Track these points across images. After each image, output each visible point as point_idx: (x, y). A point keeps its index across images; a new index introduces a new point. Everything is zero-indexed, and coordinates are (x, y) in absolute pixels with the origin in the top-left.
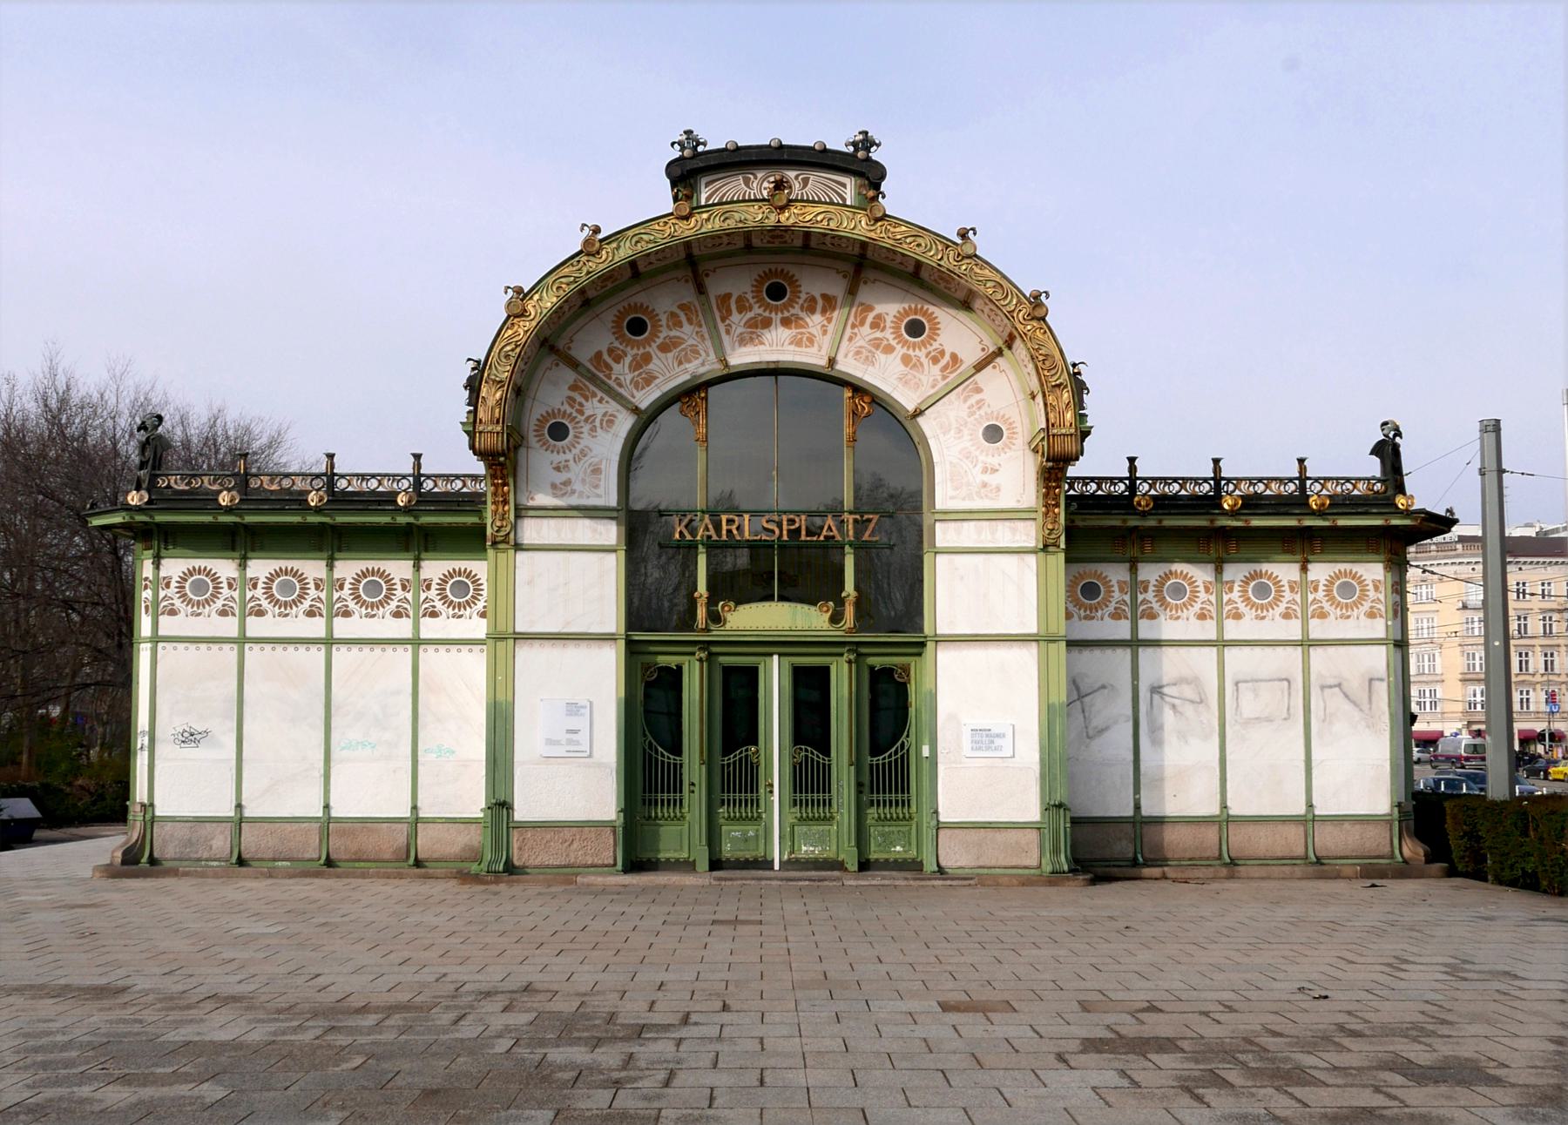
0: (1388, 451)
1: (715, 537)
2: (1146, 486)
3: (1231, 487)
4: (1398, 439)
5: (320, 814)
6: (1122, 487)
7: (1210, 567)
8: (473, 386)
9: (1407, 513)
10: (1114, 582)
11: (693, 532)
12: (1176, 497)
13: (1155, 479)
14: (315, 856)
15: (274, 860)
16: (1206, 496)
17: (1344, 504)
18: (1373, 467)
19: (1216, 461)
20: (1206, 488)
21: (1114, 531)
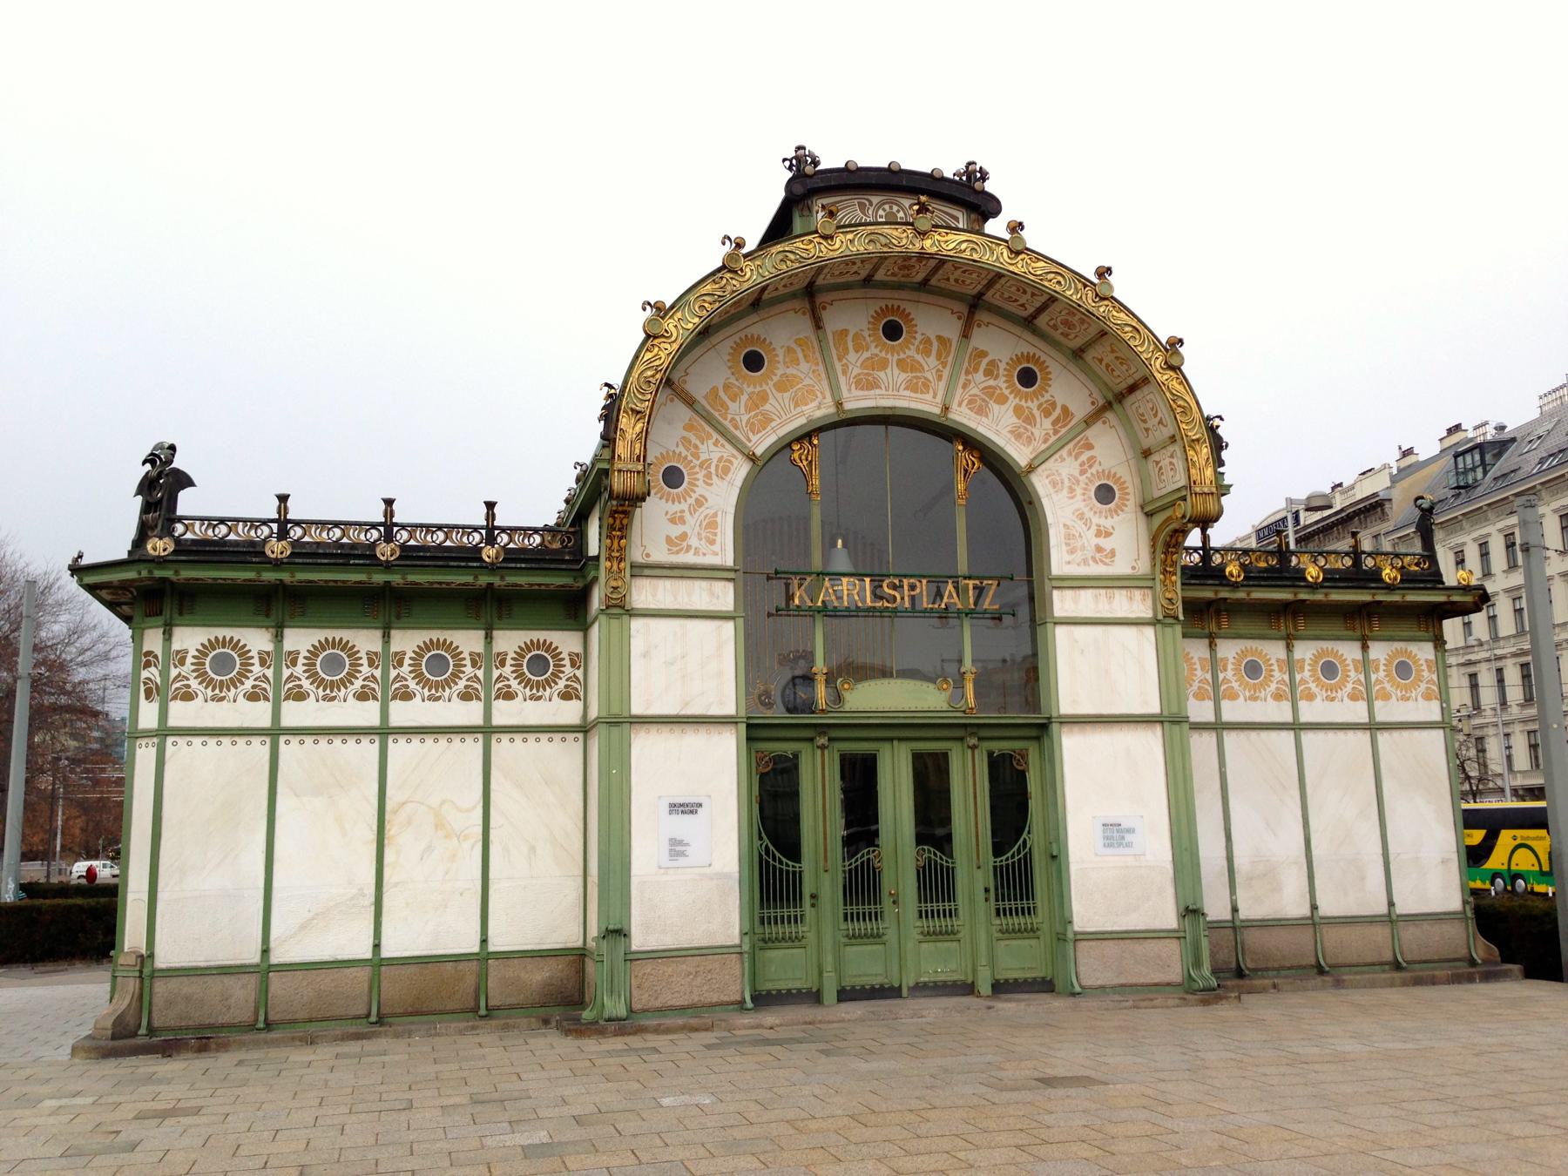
7: (1281, 645)
10: (1195, 660)
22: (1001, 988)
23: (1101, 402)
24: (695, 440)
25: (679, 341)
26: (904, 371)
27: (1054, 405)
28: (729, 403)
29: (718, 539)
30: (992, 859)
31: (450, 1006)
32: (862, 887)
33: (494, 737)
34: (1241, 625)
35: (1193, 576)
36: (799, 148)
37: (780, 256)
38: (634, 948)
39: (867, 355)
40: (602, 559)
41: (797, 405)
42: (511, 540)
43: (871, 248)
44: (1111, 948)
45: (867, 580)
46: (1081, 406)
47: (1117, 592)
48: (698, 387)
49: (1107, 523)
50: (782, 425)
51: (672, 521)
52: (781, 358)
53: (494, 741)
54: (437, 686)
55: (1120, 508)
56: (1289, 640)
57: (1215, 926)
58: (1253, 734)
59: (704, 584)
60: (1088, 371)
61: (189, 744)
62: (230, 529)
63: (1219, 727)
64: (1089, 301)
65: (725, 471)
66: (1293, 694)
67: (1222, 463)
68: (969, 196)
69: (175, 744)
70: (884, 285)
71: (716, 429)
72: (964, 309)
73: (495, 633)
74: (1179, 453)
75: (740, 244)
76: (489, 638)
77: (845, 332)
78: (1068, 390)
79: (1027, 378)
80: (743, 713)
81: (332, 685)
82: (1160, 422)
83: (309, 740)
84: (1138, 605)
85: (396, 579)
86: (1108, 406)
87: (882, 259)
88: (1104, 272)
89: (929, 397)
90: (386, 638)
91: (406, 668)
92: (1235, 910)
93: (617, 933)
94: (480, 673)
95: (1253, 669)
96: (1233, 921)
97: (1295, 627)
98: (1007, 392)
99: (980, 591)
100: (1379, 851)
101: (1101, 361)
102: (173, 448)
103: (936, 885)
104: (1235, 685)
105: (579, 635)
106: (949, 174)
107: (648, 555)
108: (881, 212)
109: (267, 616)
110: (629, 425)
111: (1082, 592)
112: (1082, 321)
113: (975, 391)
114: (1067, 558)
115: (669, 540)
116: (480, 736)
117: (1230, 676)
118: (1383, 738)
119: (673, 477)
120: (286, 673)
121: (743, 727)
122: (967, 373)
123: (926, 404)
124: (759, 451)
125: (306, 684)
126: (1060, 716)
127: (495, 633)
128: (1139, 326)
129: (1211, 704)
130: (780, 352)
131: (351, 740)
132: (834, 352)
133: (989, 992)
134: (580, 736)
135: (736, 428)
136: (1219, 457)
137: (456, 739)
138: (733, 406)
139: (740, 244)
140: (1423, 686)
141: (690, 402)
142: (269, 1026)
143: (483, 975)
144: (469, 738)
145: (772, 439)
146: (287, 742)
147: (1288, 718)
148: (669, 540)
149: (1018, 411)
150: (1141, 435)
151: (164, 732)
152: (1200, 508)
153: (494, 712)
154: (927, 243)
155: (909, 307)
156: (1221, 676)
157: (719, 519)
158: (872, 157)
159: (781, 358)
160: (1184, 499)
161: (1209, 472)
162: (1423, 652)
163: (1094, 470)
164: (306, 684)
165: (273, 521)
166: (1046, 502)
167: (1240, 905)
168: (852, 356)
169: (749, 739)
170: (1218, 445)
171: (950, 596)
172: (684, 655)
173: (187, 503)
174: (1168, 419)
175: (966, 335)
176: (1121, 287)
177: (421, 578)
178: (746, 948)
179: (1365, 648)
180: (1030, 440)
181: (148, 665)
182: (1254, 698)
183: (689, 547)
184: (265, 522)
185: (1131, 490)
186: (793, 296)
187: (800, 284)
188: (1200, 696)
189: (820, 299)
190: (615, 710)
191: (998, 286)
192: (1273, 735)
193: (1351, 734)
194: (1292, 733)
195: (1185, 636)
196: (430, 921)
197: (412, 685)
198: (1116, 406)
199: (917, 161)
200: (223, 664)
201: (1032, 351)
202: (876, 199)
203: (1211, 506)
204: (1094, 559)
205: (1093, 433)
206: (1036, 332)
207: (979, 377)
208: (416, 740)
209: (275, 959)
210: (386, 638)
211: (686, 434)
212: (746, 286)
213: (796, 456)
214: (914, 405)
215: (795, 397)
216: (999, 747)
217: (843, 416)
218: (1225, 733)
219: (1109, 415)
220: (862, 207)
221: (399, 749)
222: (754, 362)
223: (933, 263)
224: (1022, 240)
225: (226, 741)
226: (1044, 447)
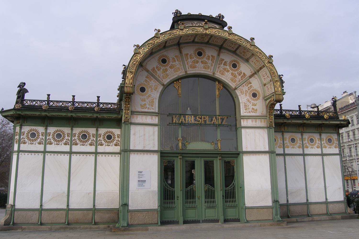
8: (124, 73)
16: (298, 115)
19: (299, 106)
21: (286, 124)
23: (253, 72)
24: (148, 81)
25: (143, 55)
27: (241, 73)
28: (158, 71)
29: (154, 105)
30: (225, 188)
32: (190, 195)
33: (98, 155)
35: (277, 117)
37: (169, 34)
38: (130, 209)
39: (193, 60)
40: (124, 110)
42: (103, 106)
43: (193, 32)
45: (193, 116)
46: (248, 73)
48: (150, 68)
51: (142, 101)
52: (171, 60)
53: (97, 156)
54: (84, 142)
55: (258, 99)
57: (281, 205)
58: (293, 157)
60: (250, 65)
62: (36, 103)
63: (284, 155)
64: (248, 46)
66: (303, 147)
67: (283, 87)
68: (219, 21)
69: (21, 154)
70: (198, 43)
71: (154, 78)
72: (218, 49)
74: (272, 84)
75: (159, 31)
76: (97, 130)
77: (187, 54)
79: (234, 66)
81: (58, 141)
82: (268, 77)
83: (52, 154)
85: (74, 115)
86: (255, 73)
87: (196, 35)
88: (252, 39)
89: (209, 70)
91: (76, 137)
92: (288, 201)
93: (125, 205)
96: (287, 204)
97: (303, 130)
98: (229, 69)
99: (222, 119)
101: (253, 61)
102: (25, 84)
103: (210, 195)
104: (289, 144)
105: (120, 129)
106: (214, 16)
107: (136, 109)
109: (44, 124)
110: (129, 76)
112: (248, 51)
114: (245, 111)
115: (141, 105)
117: (287, 142)
118: (325, 157)
119: (143, 90)
124: (165, 83)
125: (52, 140)
126: (243, 151)
127: (99, 129)
128: (261, 52)
129: (282, 149)
130: (171, 59)
131: (63, 155)
134: (119, 155)
135: (159, 77)
137: (88, 155)
138: (158, 72)
139: (159, 31)
140: (335, 144)
141: (148, 71)
142: (41, 224)
144: (91, 155)
146: (47, 155)
147: (302, 153)
148: (141, 105)
149: (232, 74)
150: (263, 80)
151: (19, 151)
152: (278, 98)
154: (207, 32)
155: (204, 48)
157: (154, 100)
158: (195, 12)
160: (273, 95)
161: (280, 89)
163: (251, 89)
164: (52, 140)
165: (46, 101)
166: (239, 97)
167: (289, 200)
168: (189, 60)
169: (161, 156)
170: (282, 82)
171: (214, 120)
172: (145, 135)
173: (27, 96)
174: (270, 76)
175: (219, 55)
176: (257, 43)
177: (80, 115)
178: (159, 210)
181: (16, 135)
182: (293, 148)
183: (146, 107)
184: (44, 101)
185: (261, 94)
186: (174, 45)
187: (176, 42)
188: (280, 147)
189: (181, 46)
190: (126, 148)
191: (226, 43)
192: (298, 157)
193: (317, 156)
194: (303, 156)
195: (275, 132)
196: (80, 200)
198: (257, 73)
199: (206, 13)
201: (236, 59)
202: (195, 22)
203: (281, 98)
205: (250, 79)
206: (236, 54)
208: (78, 155)
210: (72, 130)
213: (175, 85)
214: (205, 72)
215: (175, 70)
216: (227, 159)
217: (187, 75)
218: (286, 156)
219: (256, 75)
220: (192, 24)
221: (74, 157)
222: (164, 61)
223: (209, 36)
224: (231, 31)
225: (33, 154)
226: (239, 83)
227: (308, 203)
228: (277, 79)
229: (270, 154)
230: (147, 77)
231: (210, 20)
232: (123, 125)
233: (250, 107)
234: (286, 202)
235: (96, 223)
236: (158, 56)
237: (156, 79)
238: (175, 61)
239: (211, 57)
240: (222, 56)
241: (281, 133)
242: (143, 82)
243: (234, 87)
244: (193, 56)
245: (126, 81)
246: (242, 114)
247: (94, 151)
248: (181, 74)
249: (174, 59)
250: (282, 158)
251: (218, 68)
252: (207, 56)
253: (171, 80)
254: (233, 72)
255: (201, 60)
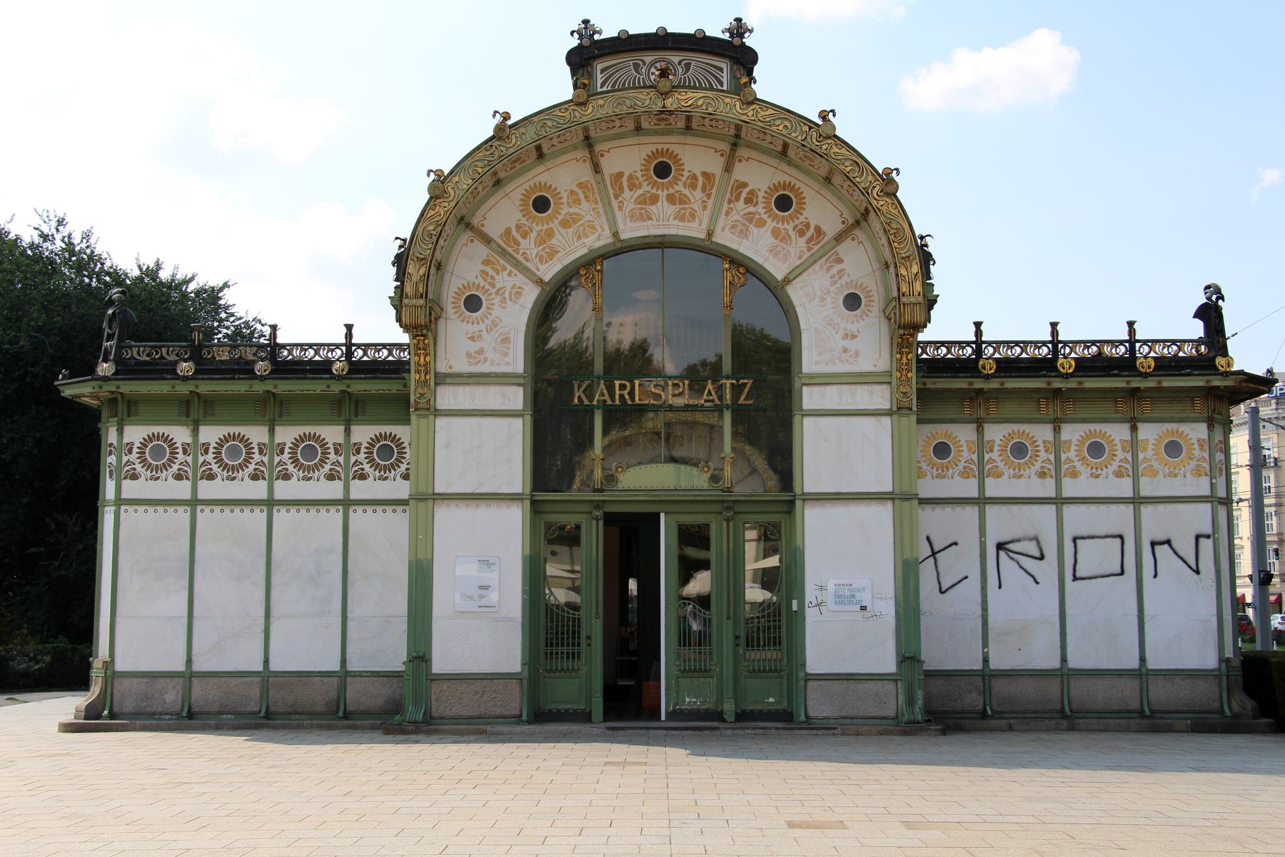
0: (1210, 314)
1: (609, 402)
2: (991, 350)
3: (1068, 350)
4: (1220, 302)
5: (261, 669)
6: (969, 350)
9: (1228, 374)
11: (591, 398)
12: (1018, 359)
13: (999, 343)
14: (256, 709)
15: (221, 713)
16: (1044, 359)
17: (1167, 366)
18: (1197, 329)
20: (1044, 350)
22: (743, 717)
24: (491, 272)
26: (674, 204)
27: (808, 226)
29: (511, 352)
31: (319, 709)
33: (353, 508)
34: (1009, 409)
36: (586, 22)
38: (434, 671)
39: (640, 192)
41: (579, 238)
44: (838, 686)
46: (832, 226)
47: (859, 387)
48: (494, 228)
49: (853, 328)
50: (569, 253)
51: (472, 339)
52: (565, 200)
54: (309, 469)
56: (1057, 423)
59: (497, 388)
61: (136, 511)
65: (518, 293)
69: (126, 511)
72: (725, 147)
73: (353, 428)
75: (506, 116)
76: (348, 432)
78: (821, 211)
79: (784, 203)
80: (528, 491)
84: (880, 397)
86: (857, 223)
90: (272, 432)
91: (286, 456)
92: (986, 660)
93: (420, 657)
94: (341, 459)
95: (1019, 450)
98: (765, 217)
99: (737, 390)
100: (1135, 611)
108: (653, 70)
111: (829, 388)
113: (737, 217)
115: (469, 355)
116: (341, 508)
119: (473, 303)
120: (201, 459)
121: (528, 503)
122: (730, 202)
123: (694, 231)
124: (547, 278)
125: (215, 467)
128: (860, 161)
129: (975, 481)
130: (564, 195)
132: (611, 192)
133: (733, 719)
135: (527, 260)
136: (928, 272)
137: (323, 509)
139: (506, 116)
141: (487, 240)
142: (191, 715)
143: (343, 688)
144: (333, 509)
145: (558, 267)
146: (202, 511)
147: (1051, 493)
148: (469, 355)
149: (775, 233)
151: (120, 502)
153: (352, 489)
155: (676, 149)
156: (987, 457)
157: (512, 336)
159: (565, 200)
161: (918, 286)
162: (1196, 432)
163: (843, 281)
164: (215, 467)
168: (627, 194)
170: (926, 259)
175: (728, 169)
178: (526, 674)
179: (1134, 429)
180: (785, 258)
181: (110, 454)
183: (486, 360)
185: (875, 298)
190: (422, 489)
193: (1113, 507)
194: (1054, 507)
197: (291, 468)
198: (863, 223)
200: (158, 452)
203: (919, 318)
204: (840, 359)
205: (841, 249)
206: (789, 163)
207: (741, 205)
208: (293, 510)
209: (198, 666)
210: (272, 432)
211: (484, 268)
212: (511, 151)
214: (681, 233)
217: (619, 245)
218: (987, 507)
219: (857, 232)
220: (636, 67)
221: (281, 516)
222: (541, 205)
225: (161, 509)
226: (799, 262)
227: (1065, 670)
228: (908, 249)
229: (897, 502)
230: (487, 262)
231: (697, 43)
232: (413, 418)
233: (835, 343)
234: (979, 666)
235: (347, 716)
236: (521, 190)
237: (517, 264)
238: (578, 202)
239: (701, 179)
240: (741, 172)
241: (975, 426)
242: (472, 279)
243: (780, 277)
244: (641, 179)
245: (408, 289)
246: (806, 368)
247: (341, 497)
248: (598, 244)
249: (576, 194)
250: (972, 512)
251: (727, 214)
252: (686, 174)
253: (565, 267)
254: (780, 225)
255: (666, 192)
